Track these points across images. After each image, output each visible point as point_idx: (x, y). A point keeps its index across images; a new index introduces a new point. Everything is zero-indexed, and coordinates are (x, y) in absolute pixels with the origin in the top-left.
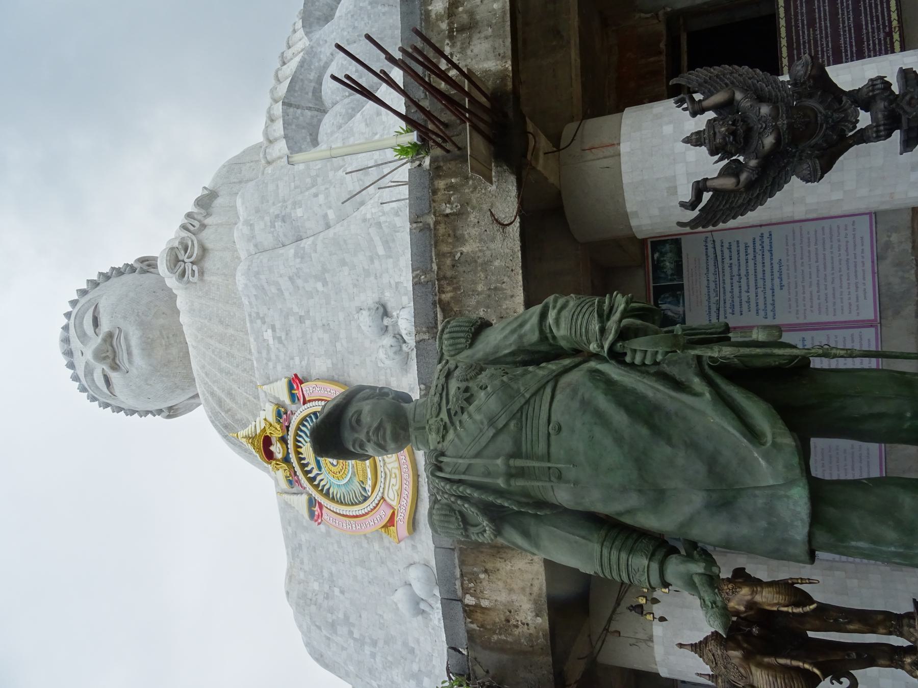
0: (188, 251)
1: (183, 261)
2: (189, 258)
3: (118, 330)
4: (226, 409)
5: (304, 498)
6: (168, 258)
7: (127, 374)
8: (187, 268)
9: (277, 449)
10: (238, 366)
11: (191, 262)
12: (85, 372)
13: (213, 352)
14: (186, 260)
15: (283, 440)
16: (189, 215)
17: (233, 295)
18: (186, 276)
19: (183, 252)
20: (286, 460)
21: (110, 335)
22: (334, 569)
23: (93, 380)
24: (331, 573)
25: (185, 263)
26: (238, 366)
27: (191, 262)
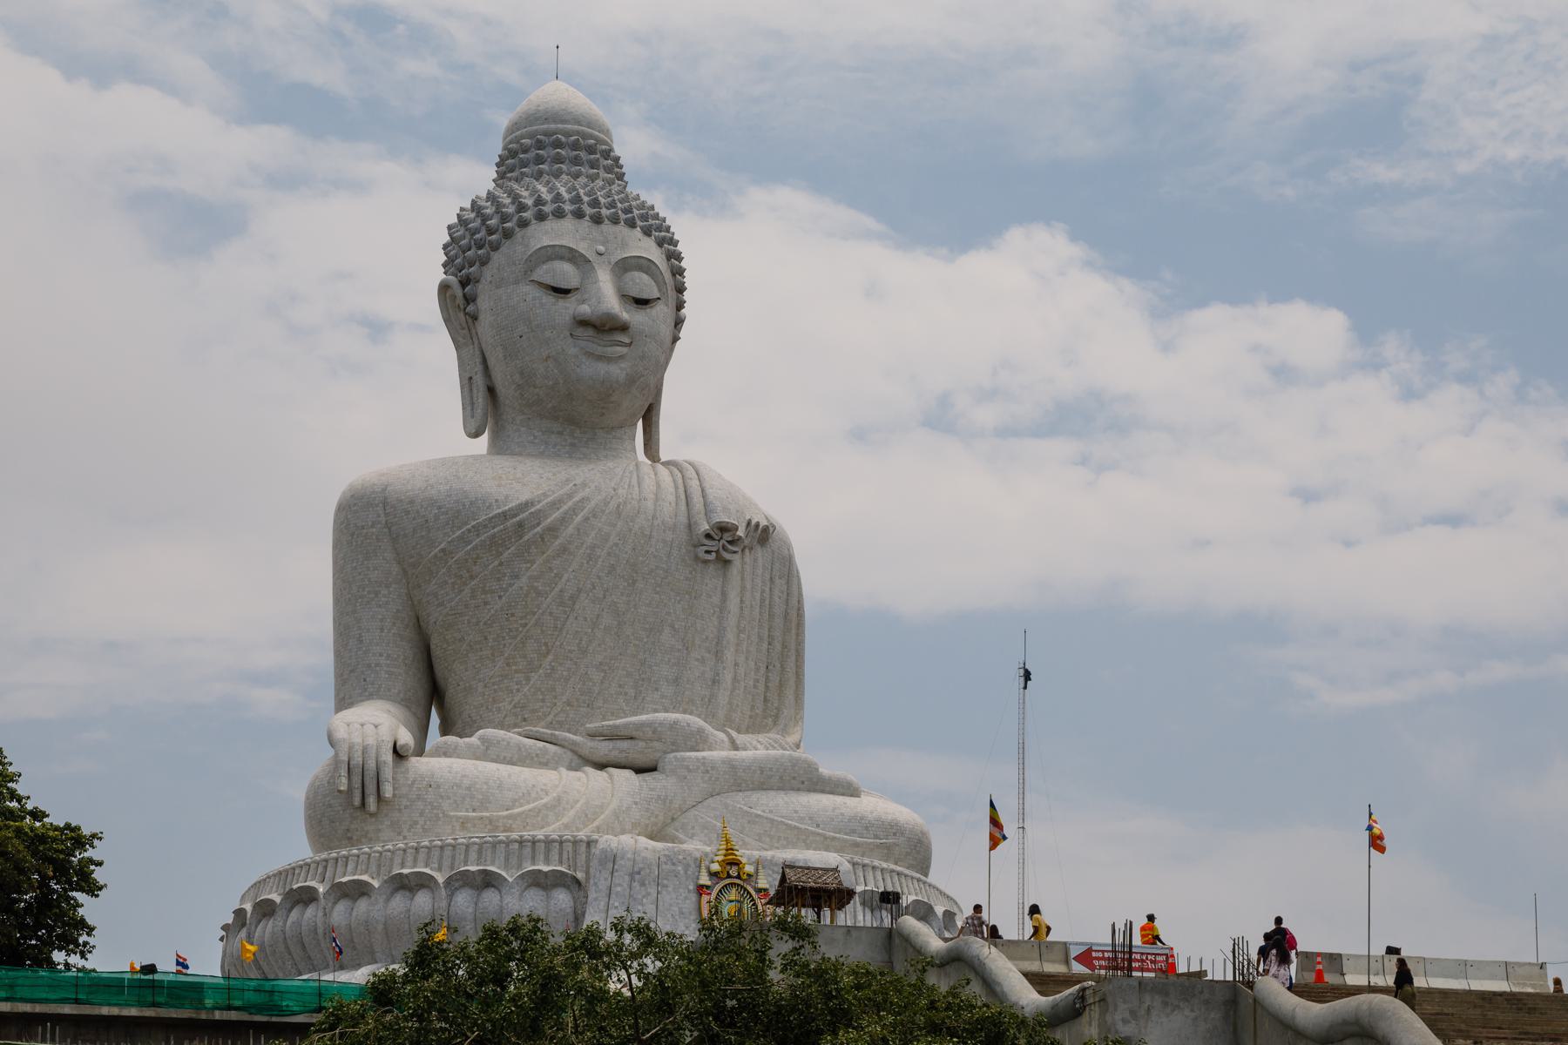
0: (730, 547)
1: (721, 538)
2: (724, 547)
3: (627, 340)
4: (544, 536)
5: (709, 883)
6: (730, 525)
7: (568, 334)
8: (713, 543)
9: (734, 872)
10: (599, 577)
11: (718, 550)
12: (576, 251)
13: (616, 545)
14: (722, 542)
15: (739, 877)
16: (757, 525)
17: (678, 598)
18: (706, 542)
19: (730, 539)
20: (729, 876)
21: (624, 328)
22: (670, 889)
23: (562, 258)
24: (667, 887)
25: (719, 541)
26: (599, 577)
27: (718, 550)
